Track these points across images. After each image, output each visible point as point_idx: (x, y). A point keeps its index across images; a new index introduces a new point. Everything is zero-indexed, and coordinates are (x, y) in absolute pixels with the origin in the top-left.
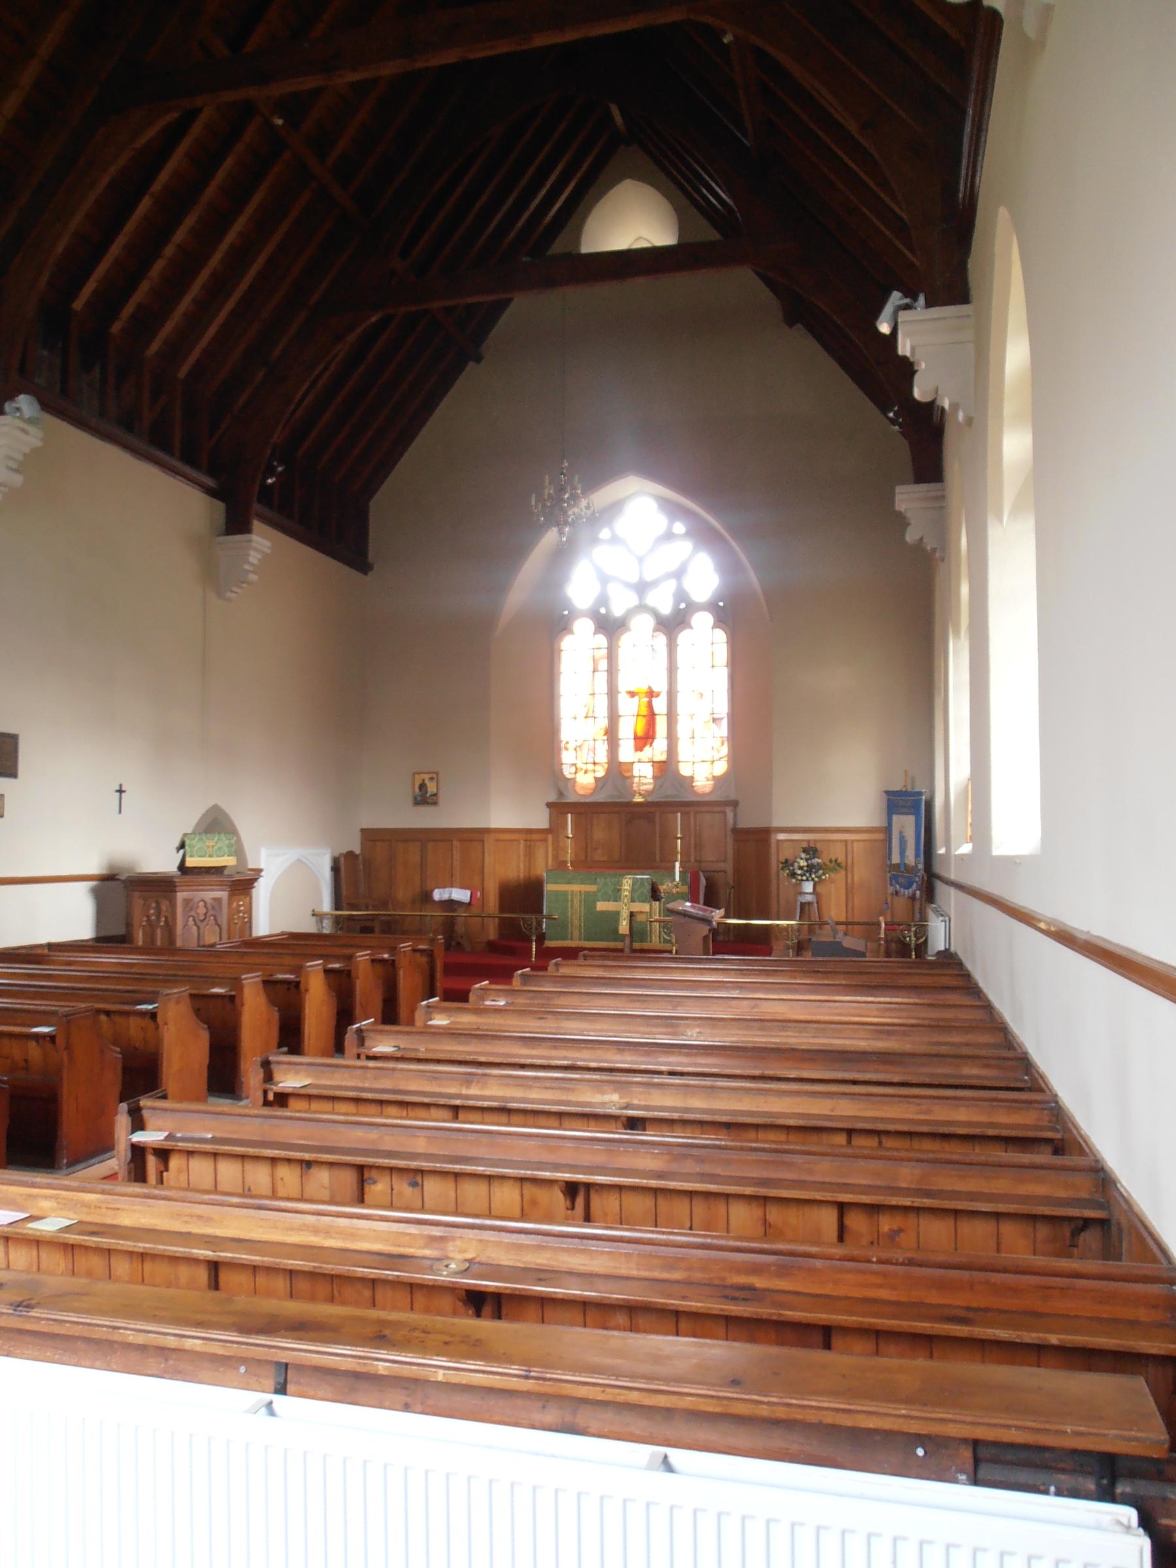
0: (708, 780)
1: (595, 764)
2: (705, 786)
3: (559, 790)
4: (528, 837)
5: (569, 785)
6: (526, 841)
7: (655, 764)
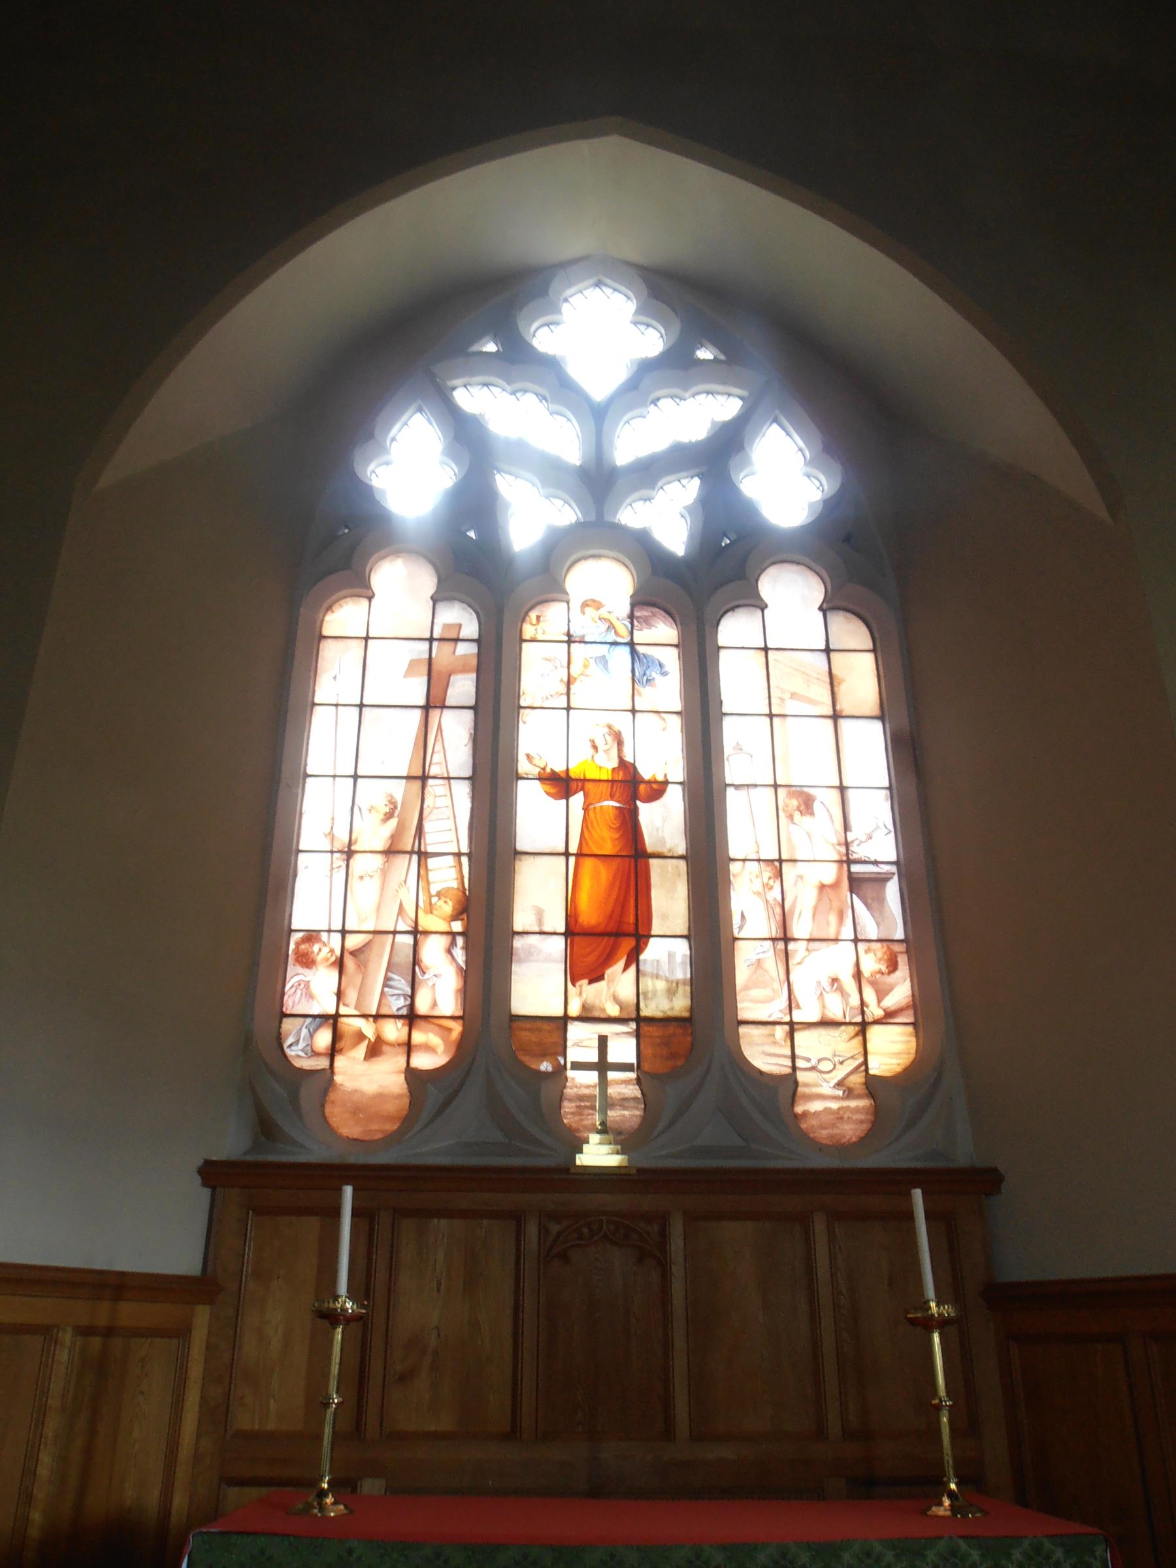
0: (850, 1093)
1: (412, 1018)
2: (839, 1116)
3: (259, 1108)
4: (102, 1312)
5: (307, 1096)
6: (85, 1331)
7: (645, 1028)
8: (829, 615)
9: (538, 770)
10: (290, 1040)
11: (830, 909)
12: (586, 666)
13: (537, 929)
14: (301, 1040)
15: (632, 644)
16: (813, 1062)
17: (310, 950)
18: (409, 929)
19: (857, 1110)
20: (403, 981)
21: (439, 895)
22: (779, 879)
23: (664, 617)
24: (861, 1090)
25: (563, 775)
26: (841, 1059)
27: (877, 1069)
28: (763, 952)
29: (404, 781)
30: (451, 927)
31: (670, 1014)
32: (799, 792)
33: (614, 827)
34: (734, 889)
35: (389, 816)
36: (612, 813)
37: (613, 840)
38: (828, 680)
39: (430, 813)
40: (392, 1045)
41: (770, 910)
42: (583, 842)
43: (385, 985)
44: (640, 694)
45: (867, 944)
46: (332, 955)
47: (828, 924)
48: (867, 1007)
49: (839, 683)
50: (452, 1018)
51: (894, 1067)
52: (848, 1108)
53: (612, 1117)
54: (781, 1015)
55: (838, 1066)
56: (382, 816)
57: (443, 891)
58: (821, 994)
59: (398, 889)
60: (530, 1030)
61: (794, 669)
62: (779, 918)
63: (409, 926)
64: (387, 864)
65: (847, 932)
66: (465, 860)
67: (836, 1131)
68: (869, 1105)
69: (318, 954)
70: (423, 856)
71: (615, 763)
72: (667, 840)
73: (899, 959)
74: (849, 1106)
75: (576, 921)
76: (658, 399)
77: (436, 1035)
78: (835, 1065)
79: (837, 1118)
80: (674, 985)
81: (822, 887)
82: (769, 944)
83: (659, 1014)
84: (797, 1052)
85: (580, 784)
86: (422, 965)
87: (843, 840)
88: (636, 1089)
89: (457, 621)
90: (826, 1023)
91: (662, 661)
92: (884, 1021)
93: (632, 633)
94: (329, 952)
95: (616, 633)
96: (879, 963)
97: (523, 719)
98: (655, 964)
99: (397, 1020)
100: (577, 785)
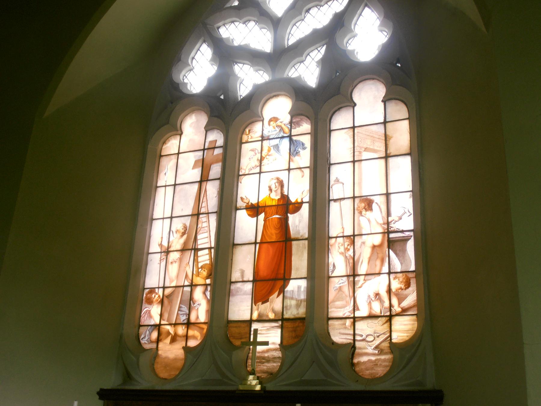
1: (188, 324)
2: (375, 364)
7: (286, 324)
8: (387, 104)
9: (246, 204)
10: (143, 336)
11: (377, 258)
12: (269, 151)
13: (241, 280)
14: (146, 336)
15: (290, 137)
16: (364, 337)
17: (151, 296)
18: (189, 284)
19: (384, 360)
20: (186, 308)
21: (202, 267)
22: (353, 245)
23: (306, 120)
24: (387, 350)
25: (256, 205)
26: (378, 335)
27: (396, 339)
28: (342, 283)
29: (190, 217)
30: (206, 282)
31: (297, 316)
32: (365, 199)
33: (276, 227)
34: (330, 252)
35: (183, 234)
36: (276, 221)
37: (276, 234)
38: (384, 138)
39: (200, 230)
40: (180, 336)
41: (348, 261)
42: (263, 237)
43: (179, 310)
44: (293, 161)
45: (395, 275)
46: (159, 299)
47: (376, 266)
48: (393, 307)
49: (390, 139)
50: (204, 323)
51: (405, 337)
52: (380, 360)
53: (269, 366)
54: (349, 314)
55: (376, 338)
56: (181, 234)
57: (204, 266)
58: (370, 302)
59: (186, 267)
60: (236, 327)
61: (367, 135)
62: (351, 265)
63: (189, 283)
64: (182, 256)
65: (385, 269)
66: (213, 250)
67: (373, 371)
68: (391, 357)
69: (154, 298)
70: (196, 250)
71: (279, 197)
72: (300, 231)
73: (411, 281)
74: (381, 358)
75: (258, 275)
76: (310, 9)
77: (197, 331)
78: (375, 338)
79: (374, 365)
80: (300, 302)
81: (374, 247)
82: (345, 279)
83: (292, 317)
84: (357, 332)
85: (263, 209)
86: (194, 300)
87: (386, 221)
88: (279, 353)
89: (215, 139)
90: (372, 317)
91: (304, 142)
92: (401, 314)
93: (291, 131)
94: (158, 297)
95: (284, 132)
96: (401, 284)
97: (240, 181)
98: (292, 293)
99: (183, 326)
100: (262, 209)
